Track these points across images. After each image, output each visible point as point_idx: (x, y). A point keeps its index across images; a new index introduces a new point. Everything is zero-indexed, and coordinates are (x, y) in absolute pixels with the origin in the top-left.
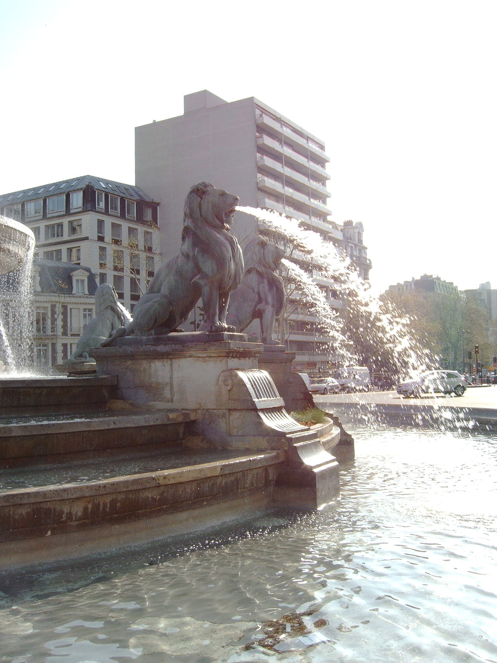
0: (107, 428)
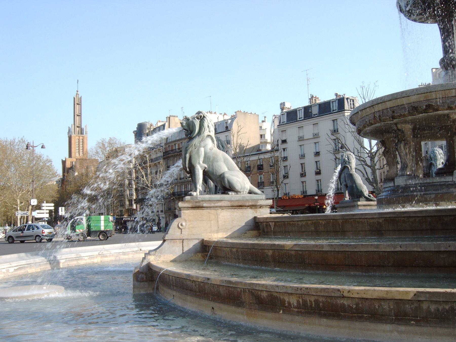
0: (393, 250)
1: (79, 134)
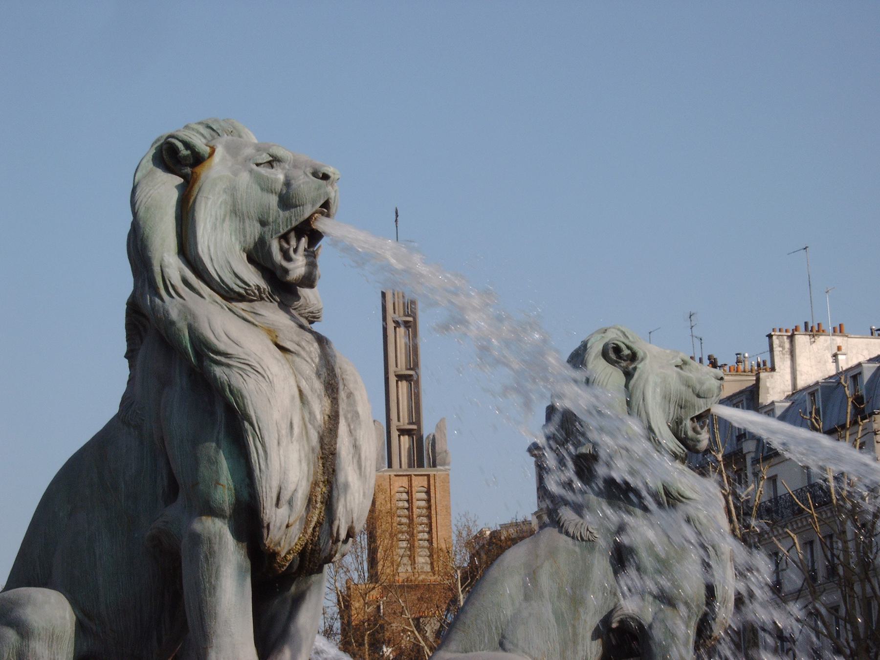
1: (410, 465)
